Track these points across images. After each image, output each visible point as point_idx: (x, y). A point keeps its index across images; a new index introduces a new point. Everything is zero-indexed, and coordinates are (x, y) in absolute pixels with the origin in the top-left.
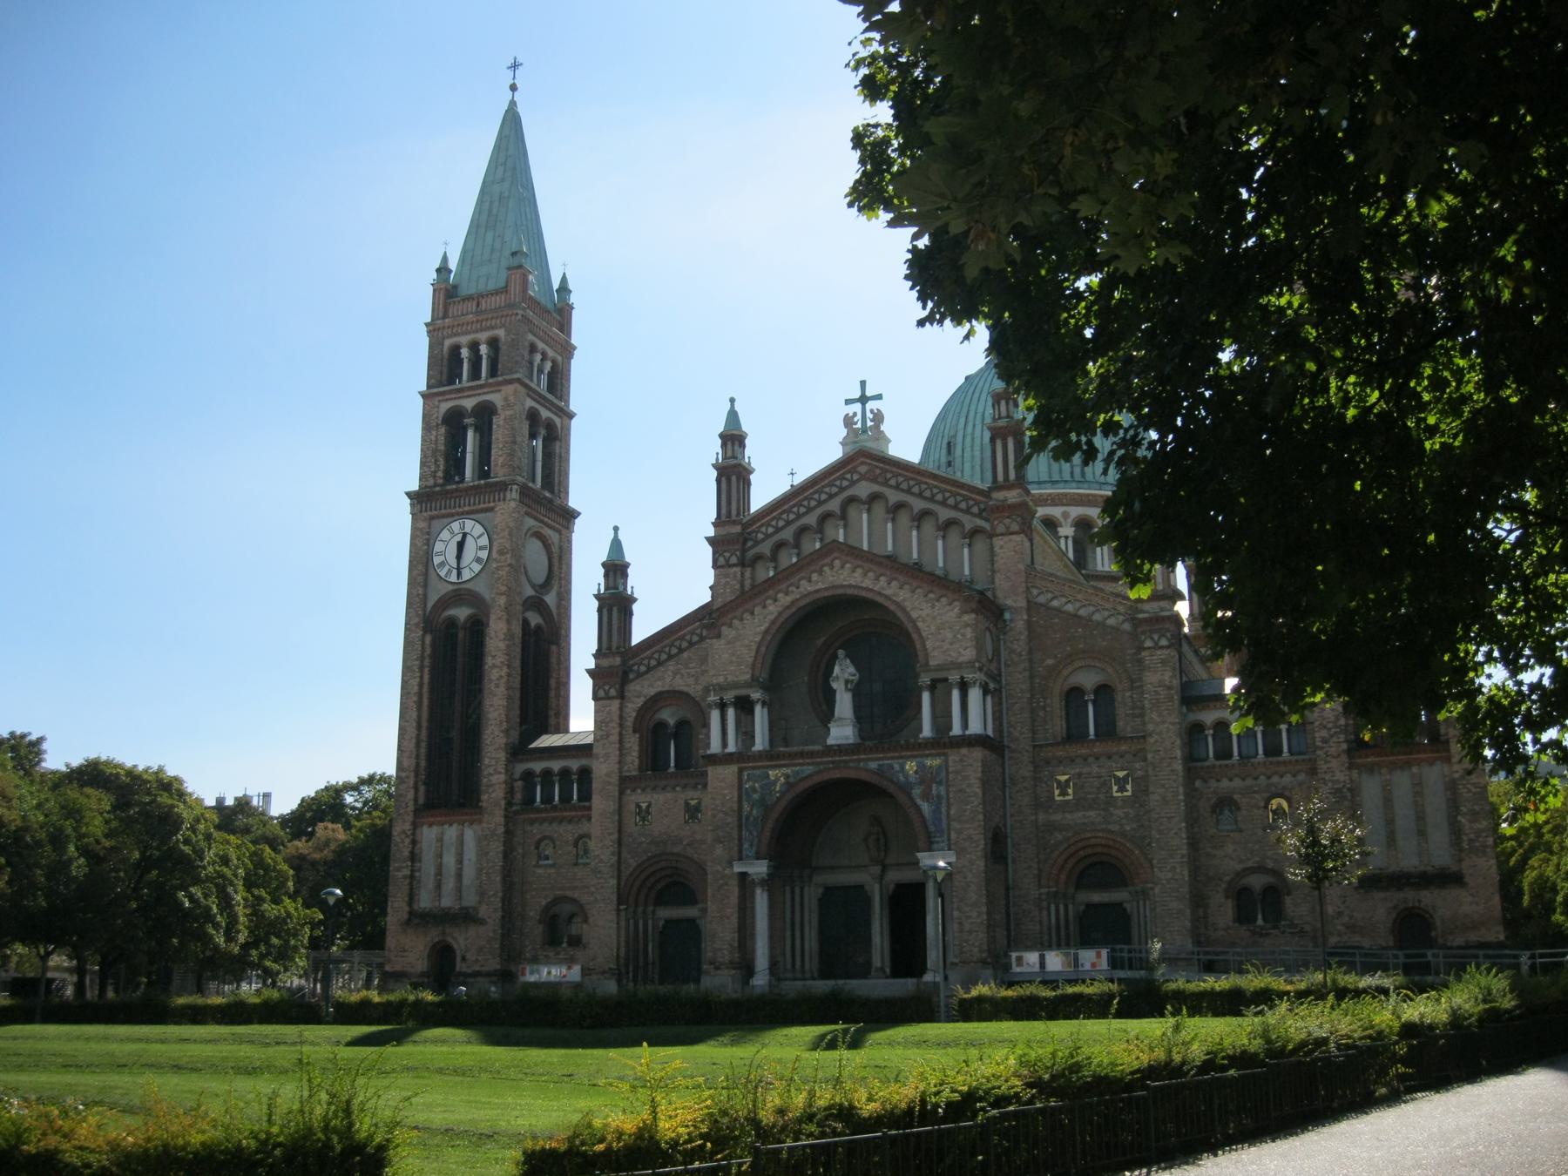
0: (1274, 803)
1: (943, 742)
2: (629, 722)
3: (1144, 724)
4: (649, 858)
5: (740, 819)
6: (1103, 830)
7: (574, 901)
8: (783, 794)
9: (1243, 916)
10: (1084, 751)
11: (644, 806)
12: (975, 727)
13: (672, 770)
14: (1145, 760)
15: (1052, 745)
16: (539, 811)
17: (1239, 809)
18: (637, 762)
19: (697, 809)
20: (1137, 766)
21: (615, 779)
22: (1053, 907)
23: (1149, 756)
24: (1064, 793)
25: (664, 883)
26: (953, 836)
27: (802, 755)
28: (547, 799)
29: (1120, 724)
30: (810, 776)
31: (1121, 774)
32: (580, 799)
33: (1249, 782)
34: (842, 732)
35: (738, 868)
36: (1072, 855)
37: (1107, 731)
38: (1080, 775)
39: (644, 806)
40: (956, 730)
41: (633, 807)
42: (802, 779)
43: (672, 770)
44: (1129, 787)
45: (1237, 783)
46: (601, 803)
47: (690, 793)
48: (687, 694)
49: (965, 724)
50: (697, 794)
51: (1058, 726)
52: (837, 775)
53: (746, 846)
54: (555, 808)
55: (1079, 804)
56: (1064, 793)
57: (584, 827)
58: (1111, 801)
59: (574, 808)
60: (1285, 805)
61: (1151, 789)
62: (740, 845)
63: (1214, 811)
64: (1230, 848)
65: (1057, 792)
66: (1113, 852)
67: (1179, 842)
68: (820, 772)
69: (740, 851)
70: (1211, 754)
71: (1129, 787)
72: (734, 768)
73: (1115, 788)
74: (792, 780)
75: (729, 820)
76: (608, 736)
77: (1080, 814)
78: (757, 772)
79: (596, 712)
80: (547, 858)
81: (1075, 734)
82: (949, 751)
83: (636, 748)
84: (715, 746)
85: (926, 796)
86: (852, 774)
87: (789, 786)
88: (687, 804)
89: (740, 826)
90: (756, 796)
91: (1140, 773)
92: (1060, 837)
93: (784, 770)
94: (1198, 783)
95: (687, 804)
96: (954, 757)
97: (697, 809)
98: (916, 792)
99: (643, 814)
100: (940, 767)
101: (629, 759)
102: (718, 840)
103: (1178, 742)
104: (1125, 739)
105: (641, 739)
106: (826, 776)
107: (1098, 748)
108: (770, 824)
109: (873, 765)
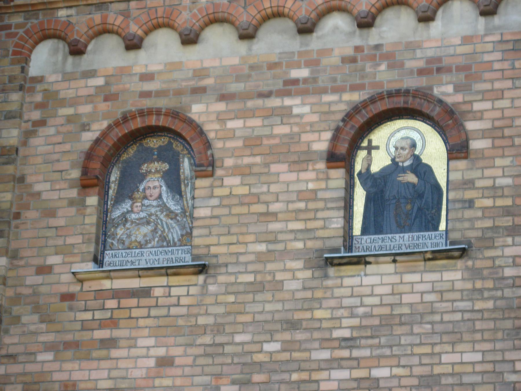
0: (385, 145)
17: (207, 167)
33: (276, 41)
45: (220, 47)
60: (433, 149)
63: (91, 180)
94: (44, 59)
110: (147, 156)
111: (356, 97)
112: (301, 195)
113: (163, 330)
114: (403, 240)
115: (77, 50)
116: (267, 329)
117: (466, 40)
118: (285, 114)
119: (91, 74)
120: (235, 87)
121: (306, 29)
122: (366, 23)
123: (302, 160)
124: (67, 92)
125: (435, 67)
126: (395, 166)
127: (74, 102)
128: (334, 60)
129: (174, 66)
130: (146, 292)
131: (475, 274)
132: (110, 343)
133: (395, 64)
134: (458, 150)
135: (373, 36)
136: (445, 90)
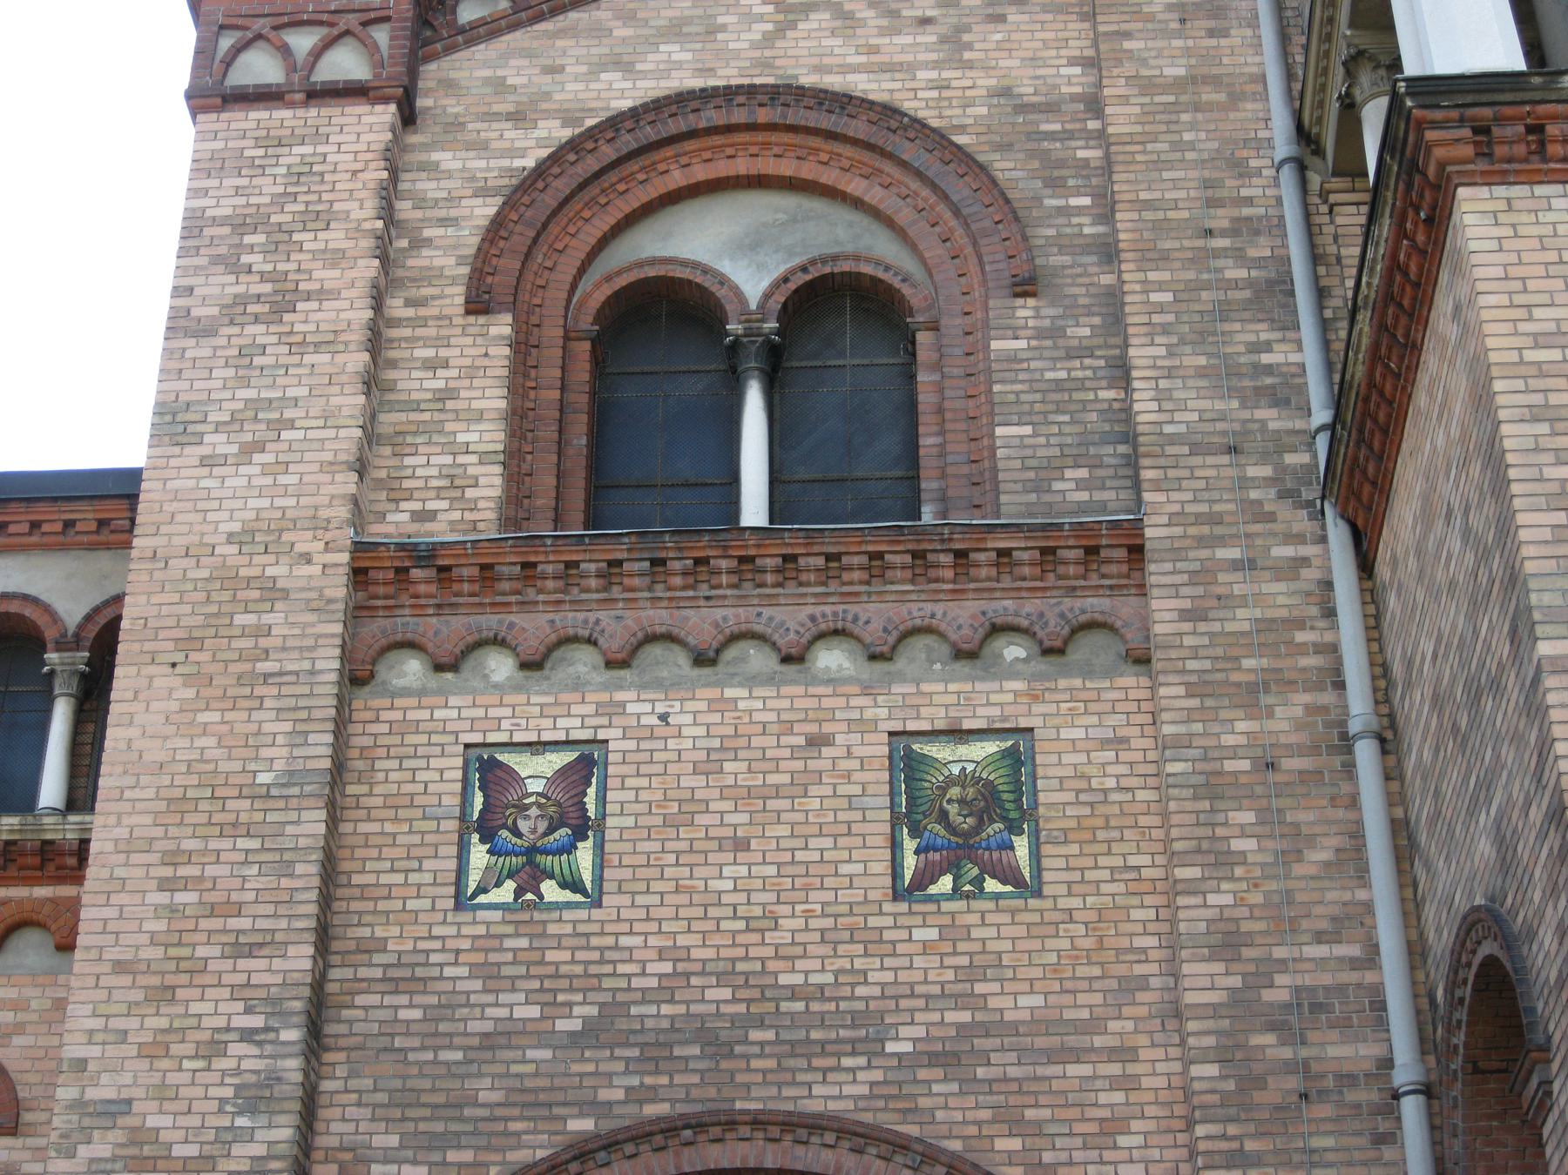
2: (446, 254)
11: (535, 772)
18: (490, 485)
39: (536, 772)
41: (444, 777)
47: (933, 694)
48: (888, 112)
50: (995, 697)
76: (283, 301)
79: (205, 167)
83: (494, 400)
88: (907, 763)
97: (1004, 800)
99: (531, 826)
101: (426, 465)
105: (523, 347)
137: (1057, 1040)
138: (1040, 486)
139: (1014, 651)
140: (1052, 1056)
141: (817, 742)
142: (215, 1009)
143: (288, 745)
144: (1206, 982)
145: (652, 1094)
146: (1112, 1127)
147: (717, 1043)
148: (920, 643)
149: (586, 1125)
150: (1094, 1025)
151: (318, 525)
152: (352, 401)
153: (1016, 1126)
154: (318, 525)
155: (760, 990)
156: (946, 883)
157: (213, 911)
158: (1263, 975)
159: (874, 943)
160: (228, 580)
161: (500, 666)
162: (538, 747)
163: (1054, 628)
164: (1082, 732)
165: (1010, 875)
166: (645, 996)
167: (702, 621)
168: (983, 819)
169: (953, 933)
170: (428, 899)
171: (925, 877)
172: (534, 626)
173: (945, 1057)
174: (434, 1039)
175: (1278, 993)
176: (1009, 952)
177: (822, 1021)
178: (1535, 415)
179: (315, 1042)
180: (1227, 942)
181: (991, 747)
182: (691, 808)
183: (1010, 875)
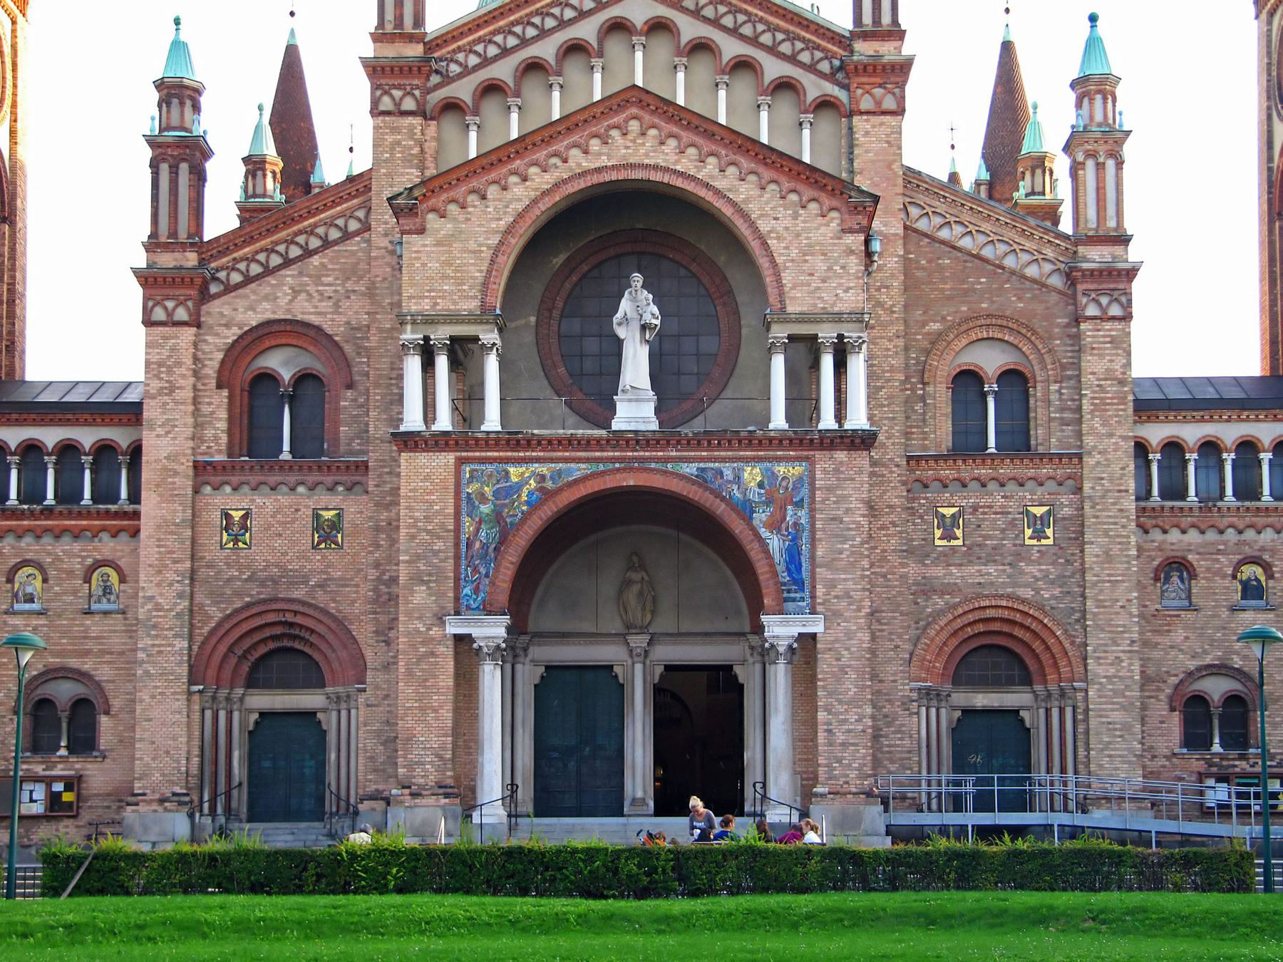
1: (805, 440)
3: (1079, 435)
4: (248, 606)
5: (457, 545)
6: (1009, 597)
7: (80, 676)
8: (534, 506)
9: (1195, 738)
10: (983, 472)
11: (237, 515)
12: (858, 419)
13: (286, 456)
14: (1079, 490)
15: (936, 458)
16: (14, 514)
19: (336, 525)
20: (1064, 500)
21: (186, 467)
22: (923, 710)
23: (1087, 486)
24: (949, 536)
25: (274, 647)
26: (820, 590)
27: (569, 443)
28: (32, 493)
29: (1038, 434)
30: (585, 478)
31: (1039, 511)
32: (95, 499)
34: (635, 411)
35: (454, 627)
36: (955, 633)
37: (1018, 442)
38: (975, 508)
39: (237, 515)
40: (827, 421)
42: (570, 485)
43: (286, 456)
44: (1049, 532)
46: (150, 505)
47: (323, 498)
49: (840, 415)
50: (335, 500)
51: (941, 433)
52: (630, 481)
53: (467, 591)
54: (48, 512)
55: (971, 553)
56: (949, 536)
57: (107, 546)
58: (1021, 553)
59: (88, 515)
61: (1087, 537)
62: (457, 588)
63: (1157, 579)
64: (1179, 635)
65: (938, 533)
66: (1018, 632)
67: (1128, 622)
68: (593, 475)
69: (457, 599)
70: (1155, 491)
71: (1049, 532)
72: (450, 458)
73: (1029, 532)
74: (549, 485)
75: (439, 545)
77: (973, 569)
78: (490, 468)
80: (30, 599)
81: (967, 444)
82: (818, 455)
84: (413, 419)
85: (775, 525)
86: (657, 482)
87: (546, 495)
88: (316, 516)
89: (457, 558)
90: (485, 509)
91: (1067, 511)
92: (940, 602)
93: (535, 467)
95: (316, 516)
96: (825, 463)
97: (336, 525)
98: (760, 517)
100: (800, 479)
101: (209, 433)
102: (418, 579)
103: (1132, 467)
104: (1051, 457)
106: (609, 483)
107: (1005, 470)
108: (513, 556)
109: (690, 469)
110: (1173, 570)
111: (1240, 557)
112: (1225, 588)
113: (1185, 628)
114: (1253, 602)
115: (1146, 532)
116: (1217, 629)
117: (1273, 541)
118: (1217, 561)
119: (1153, 541)
120: (1201, 550)
121: (1221, 532)
122: (1240, 532)
123: (1224, 577)
124: (1146, 546)
125: (1263, 549)
126: (1249, 579)
127: (1149, 550)
128: (1231, 544)
129: (1181, 541)
130: (1178, 616)
131: (1277, 616)
132: (1169, 631)
133: (1251, 547)
134: (1270, 576)
135: (1243, 537)
136: (1266, 557)
137: (343, 582)
138: (349, 444)
139: (341, 489)
140: (343, 586)
141: (297, 510)
142: (171, 576)
143: (181, 514)
144: (373, 574)
145: (262, 593)
146: (354, 601)
147: (275, 582)
148: (320, 487)
149: (248, 599)
150: (351, 579)
151: (185, 455)
152: (190, 420)
153: (334, 601)
154: (185, 455)
155: (283, 569)
156: (323, 546)
157: (169, 553)
158: (383, 573)
159: (308, 559)
160: (165, 469)
161: (228, 489)
162: (237, 510)
163: (349, 484)
164: (355, 509)
165: (337, 544)
166: (261, 571)
167: (273, 479)
168: (332, 529)
169: (324, 557)
170: (215, 545)
171: (319, 544)
172: (235, 479)
173: (320, 586)
174: (217, 580)
175: (386, 577)
176: (335, 562)
177: (297, 577)
178: (408, 508)
179: (192, 579)
180: (377, 565)
181: (333, 513)
182: (270, 526)
183: (337, 544)
